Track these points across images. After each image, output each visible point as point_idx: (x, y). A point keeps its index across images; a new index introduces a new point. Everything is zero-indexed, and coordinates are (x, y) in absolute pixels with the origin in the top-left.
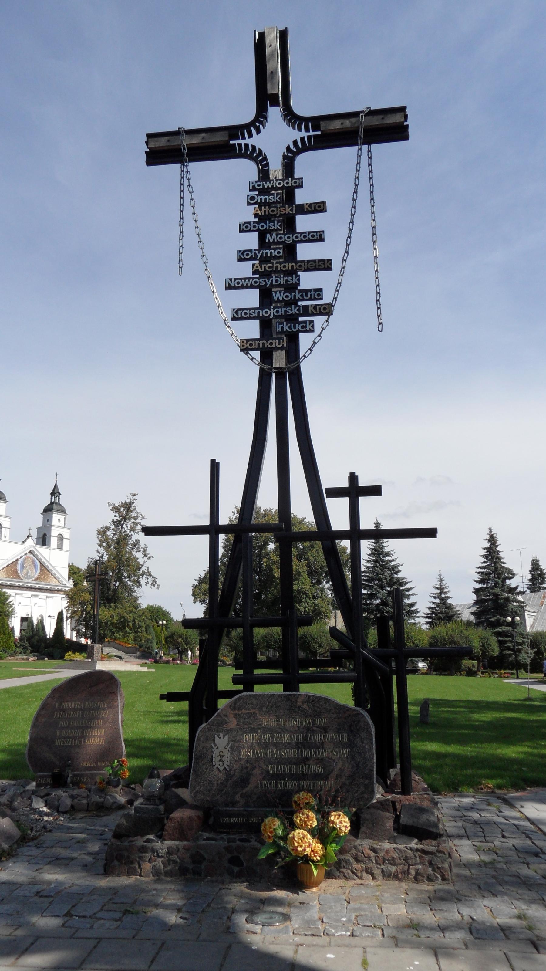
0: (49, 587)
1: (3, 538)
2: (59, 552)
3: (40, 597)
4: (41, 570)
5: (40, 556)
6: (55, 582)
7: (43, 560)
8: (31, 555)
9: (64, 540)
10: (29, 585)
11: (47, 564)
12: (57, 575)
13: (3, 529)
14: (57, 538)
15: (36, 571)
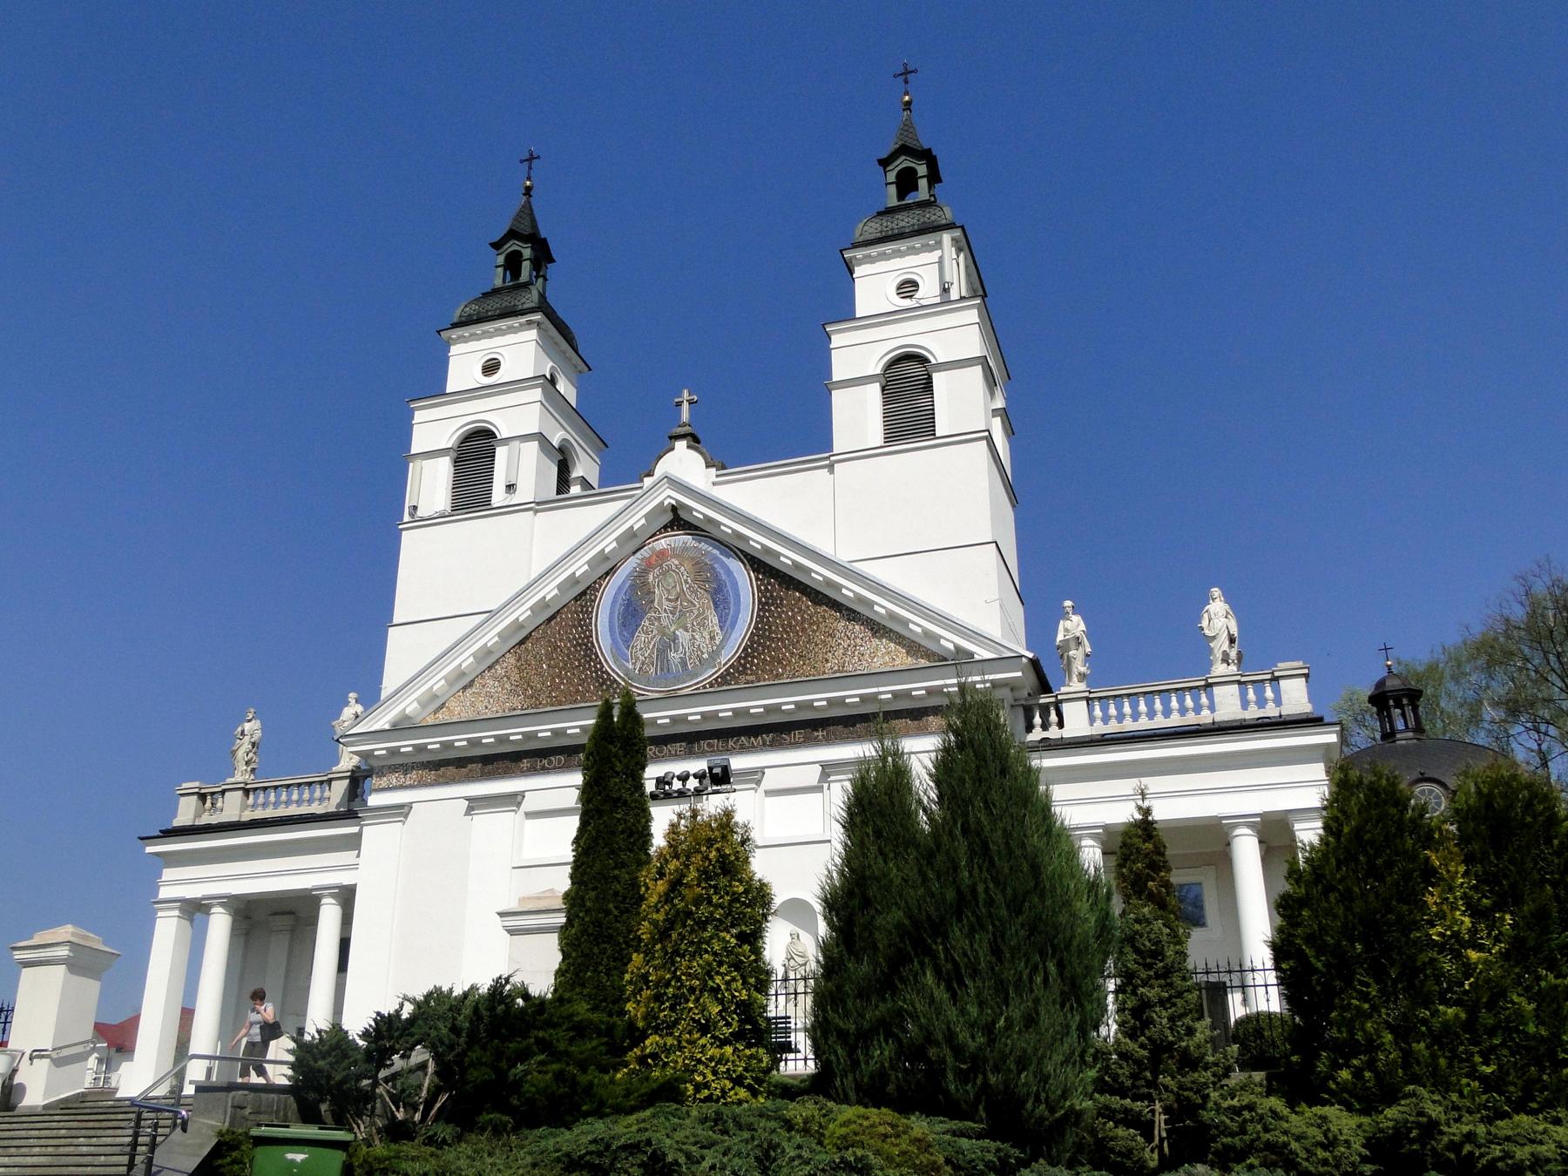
0: (852, 695)
1: (498, 496)
2: (915, 462)
3: (771, 780)
4: (764, 605)
5: (729, 525)
6: (884, 655)
7: (757, 540)
8: (682, 539)
9: (938, 379)
10: (694, 713)
11: (788, 557)
12: (882, 606)
13: (501, 453)
14: (874, 392)
15: (726, 622)
